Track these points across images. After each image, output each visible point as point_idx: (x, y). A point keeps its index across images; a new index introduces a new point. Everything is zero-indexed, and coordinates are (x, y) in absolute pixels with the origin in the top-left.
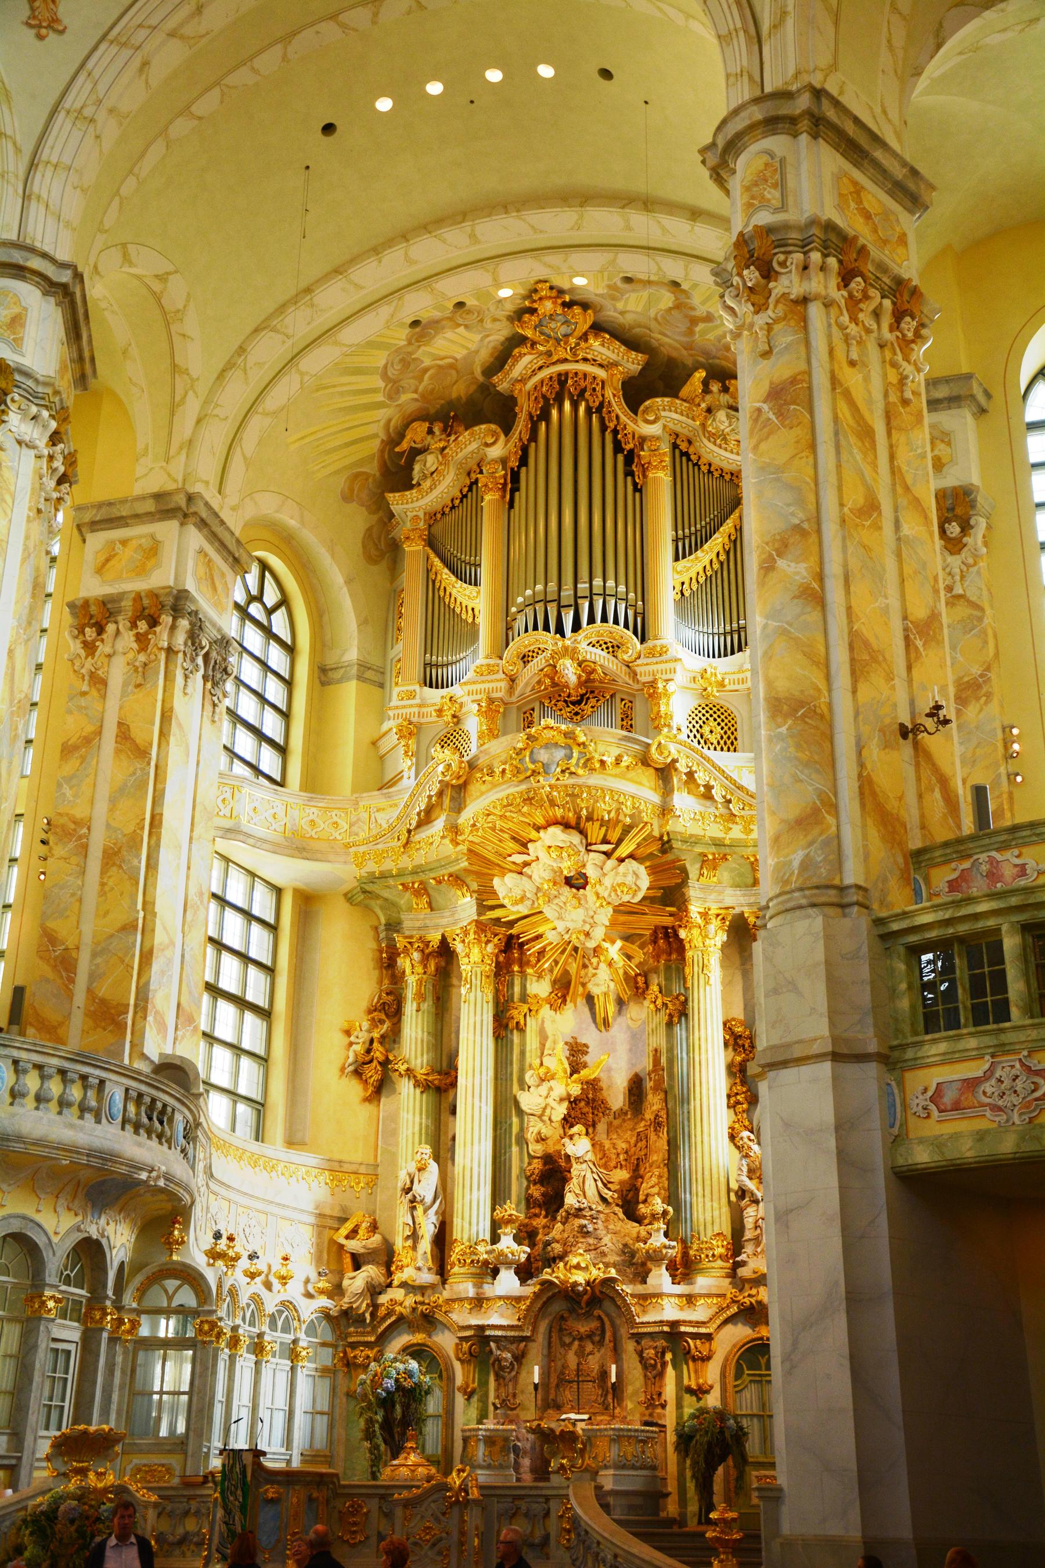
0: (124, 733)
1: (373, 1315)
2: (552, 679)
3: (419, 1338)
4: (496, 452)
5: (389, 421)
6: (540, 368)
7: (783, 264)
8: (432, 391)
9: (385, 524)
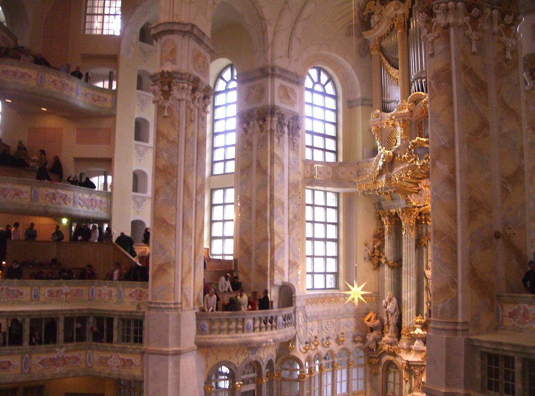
0: (259, 165)
1: (377, 348)
3: (391, 358)
4: (400, 12)
7: (437, 9)
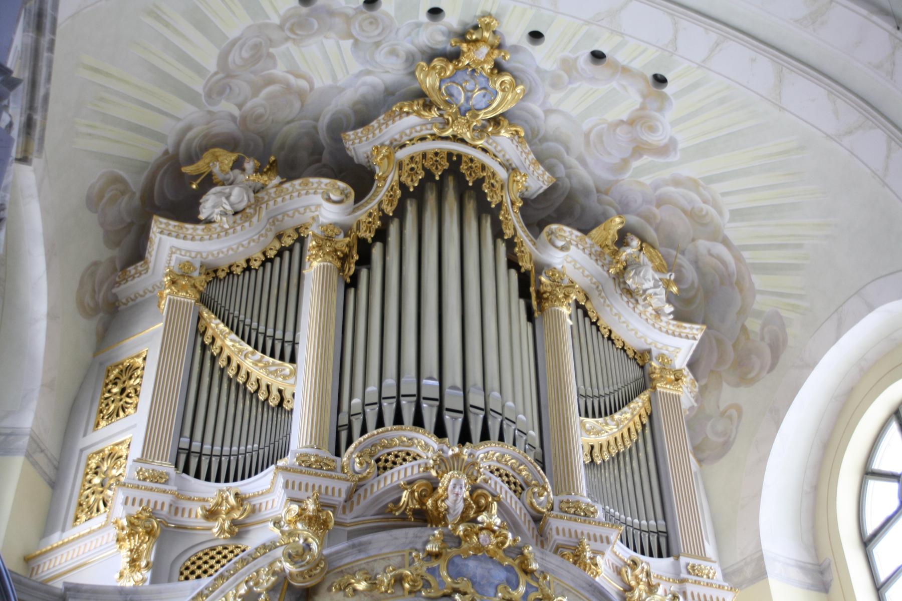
2: (422, 500)
5: (189, 128)
6: (423, 139)
8: (261, 116)
9: (115, 270)
